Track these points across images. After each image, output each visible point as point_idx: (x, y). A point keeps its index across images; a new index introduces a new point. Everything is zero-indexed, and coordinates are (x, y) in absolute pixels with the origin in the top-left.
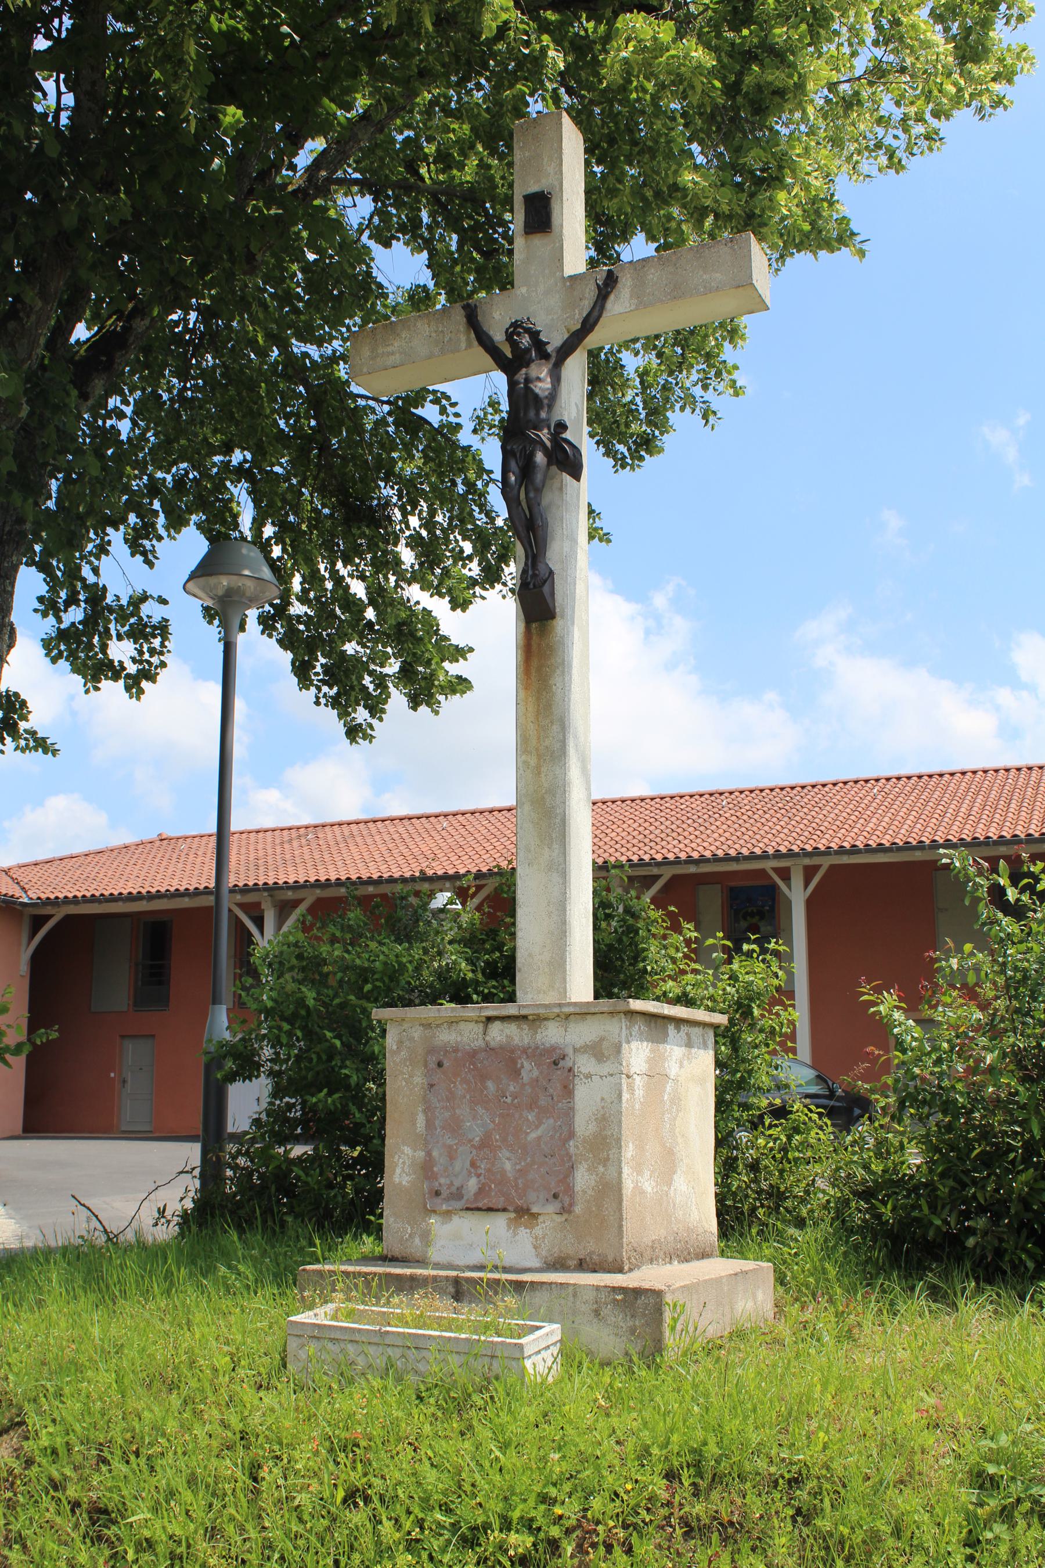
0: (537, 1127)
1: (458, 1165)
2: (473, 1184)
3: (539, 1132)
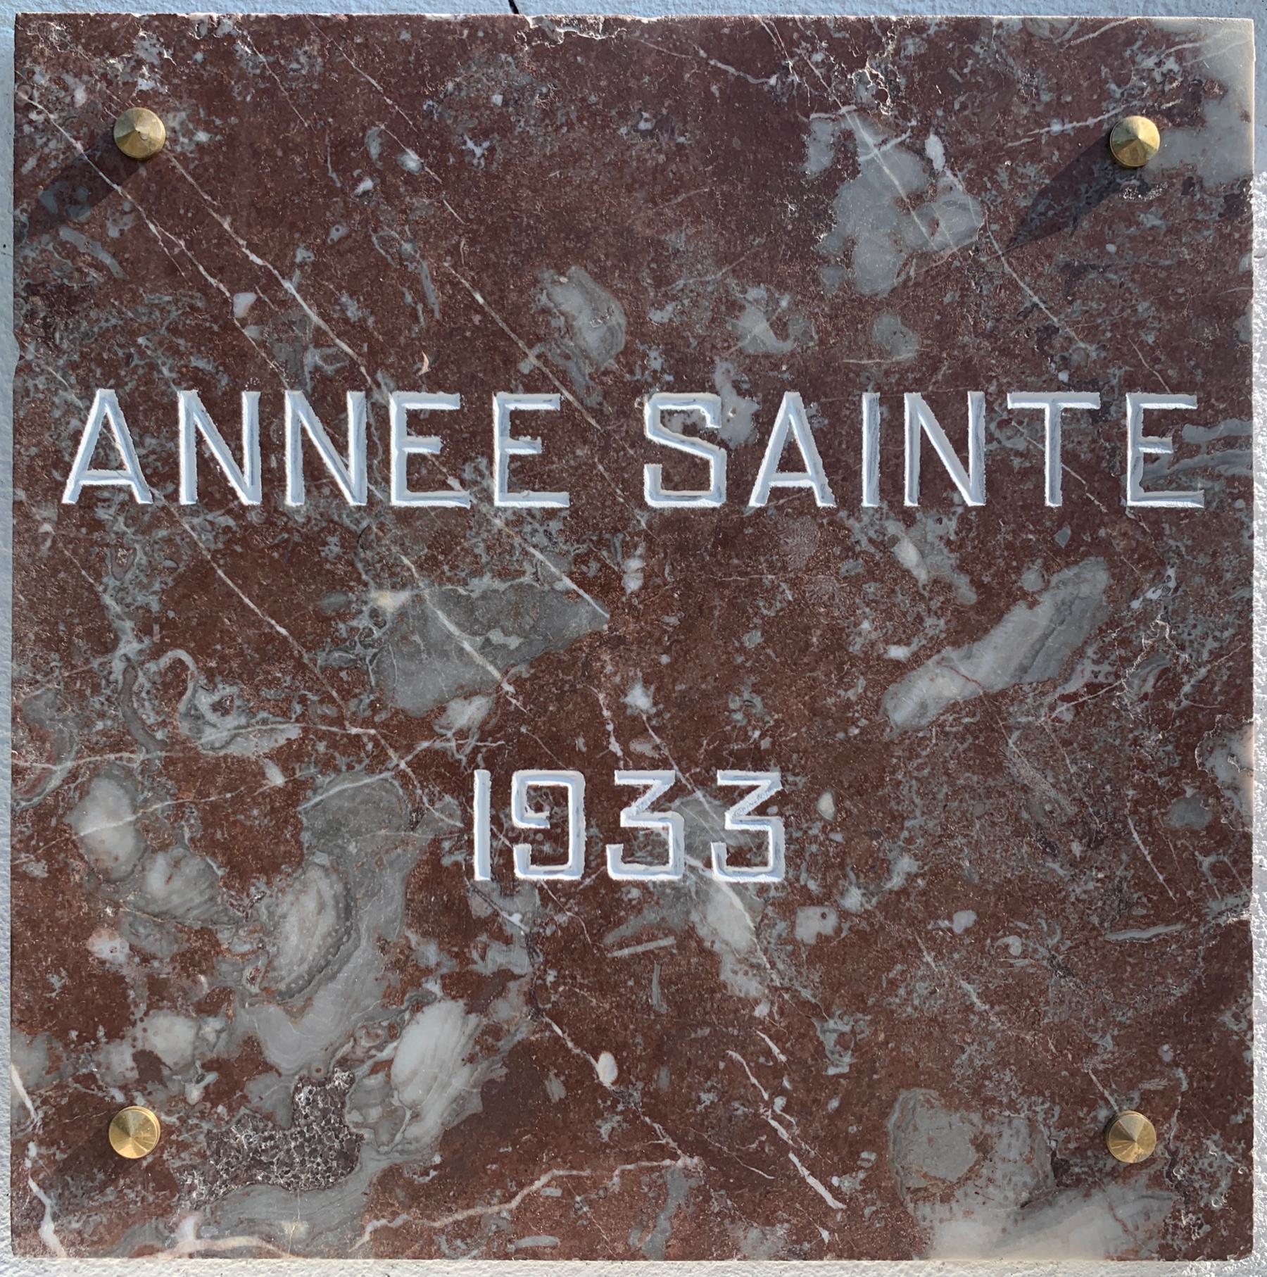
0: (969, 628)
1: (301, 917)
2: (433, 1054)
3: (989, 663)
